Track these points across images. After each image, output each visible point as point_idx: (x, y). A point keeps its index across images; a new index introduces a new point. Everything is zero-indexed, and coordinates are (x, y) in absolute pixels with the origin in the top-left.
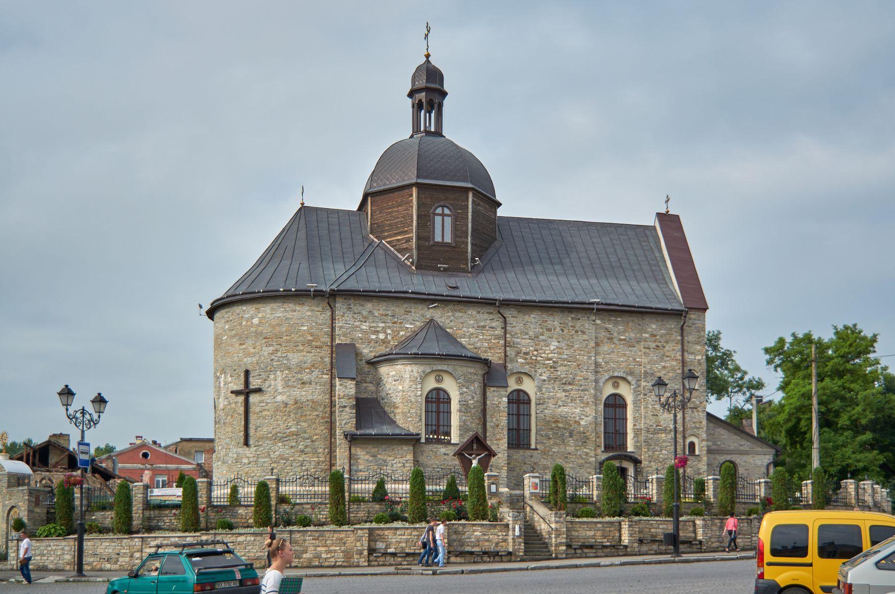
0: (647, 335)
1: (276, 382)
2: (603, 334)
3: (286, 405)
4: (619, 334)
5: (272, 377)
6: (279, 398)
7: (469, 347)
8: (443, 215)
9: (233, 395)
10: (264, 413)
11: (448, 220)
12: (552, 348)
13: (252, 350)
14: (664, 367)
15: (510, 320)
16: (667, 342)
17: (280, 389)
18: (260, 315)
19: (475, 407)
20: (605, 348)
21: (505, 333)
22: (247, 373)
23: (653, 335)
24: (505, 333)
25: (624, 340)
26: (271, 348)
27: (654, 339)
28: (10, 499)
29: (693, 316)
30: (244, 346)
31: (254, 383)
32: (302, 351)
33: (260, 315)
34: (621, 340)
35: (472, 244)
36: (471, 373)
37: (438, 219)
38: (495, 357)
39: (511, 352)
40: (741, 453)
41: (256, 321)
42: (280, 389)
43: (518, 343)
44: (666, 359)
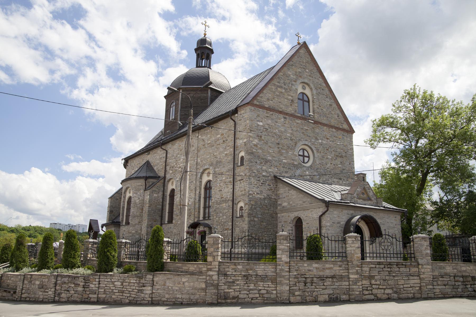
0: (219, 136)
2: (202, 143)
4: (208, 140)
7: (156, 171)
8: (173, 106)
11: (174, 107)
12: (182, 160)
14: (226, 154)
15: (170, 151)
16: (228, 136)
19: (139, 204)
20: (202, 152)
21: (166, 158)
23: (222, 134)
24: (166, 158)
25: (210, 143)
27: (222, 137)
29: (242, 112)
34: (208, 144)
35: (181, 115)
36: (139, 186)
37: (171, 109)
38: (161, 174)
39: (168, 168)
40: (304, 209)
43: (171, 162)
44: (228, 148)
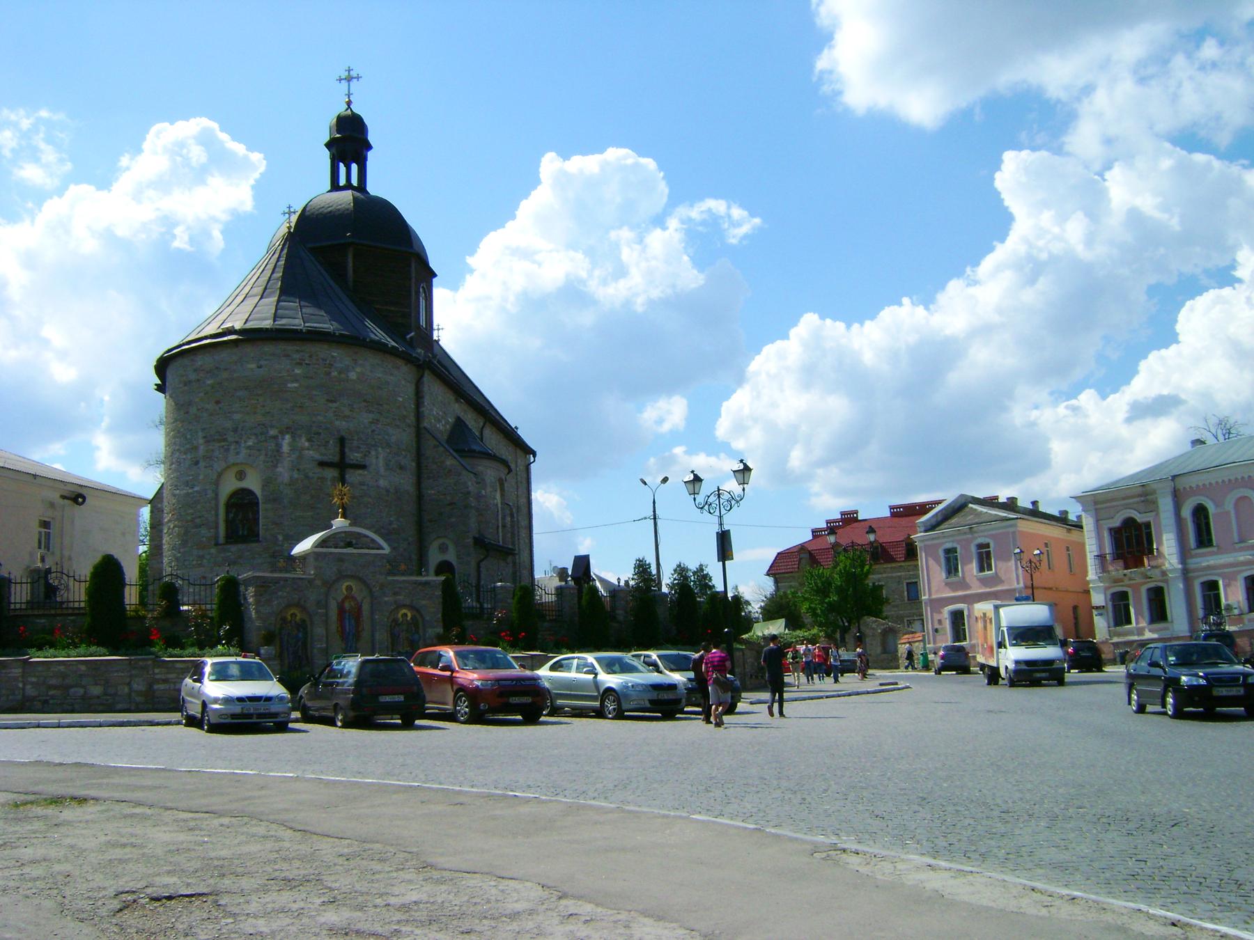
1: (378, 460)
3: (388, 491)
5: (373, 453)
6: (382, 483)
9: (318, 470)
10: (366, 499)
13: (347, 413)
17: (382, 470)
18: (358, 370)
22: (342, 441)
26: (371, 416)
28: (395, 594)
30: (335, 405)
31: (354, 456)
32: (398, 427)
33: (358, 370)
41: (353, 376)
42: (382, 470)
